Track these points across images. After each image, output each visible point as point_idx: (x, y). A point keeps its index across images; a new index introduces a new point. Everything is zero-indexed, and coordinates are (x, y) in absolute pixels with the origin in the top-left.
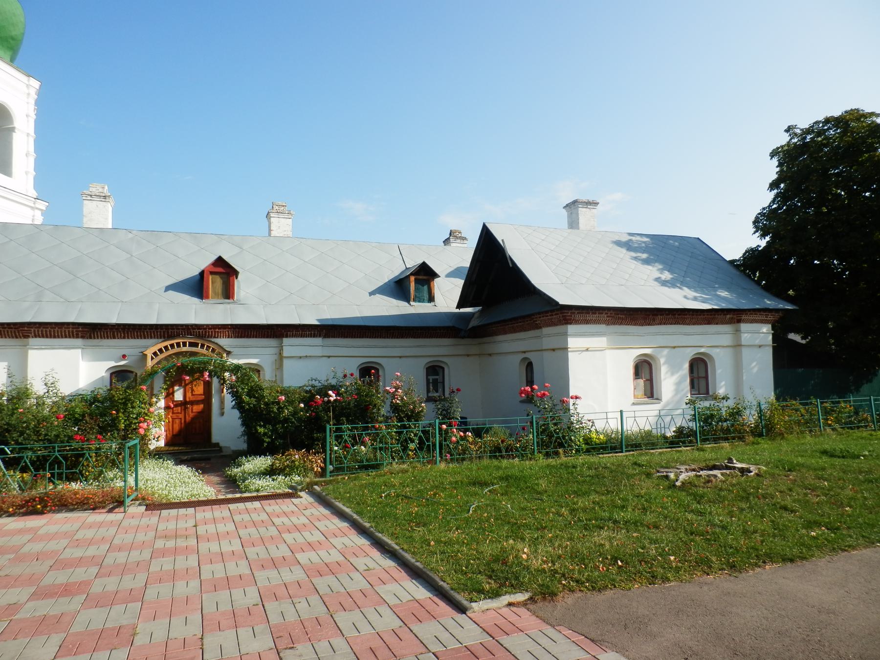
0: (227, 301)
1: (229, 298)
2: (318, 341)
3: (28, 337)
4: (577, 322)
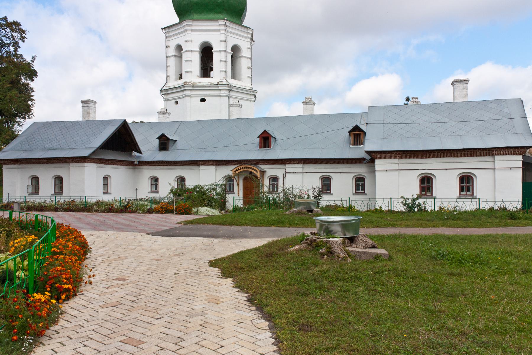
0: (265, 149)
1: (269, 148)
2: (301, 166)
3: (200, 165)
4: (380, 158)
